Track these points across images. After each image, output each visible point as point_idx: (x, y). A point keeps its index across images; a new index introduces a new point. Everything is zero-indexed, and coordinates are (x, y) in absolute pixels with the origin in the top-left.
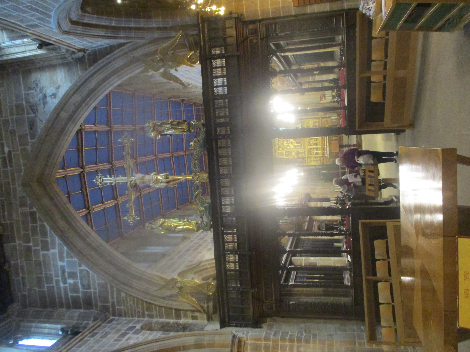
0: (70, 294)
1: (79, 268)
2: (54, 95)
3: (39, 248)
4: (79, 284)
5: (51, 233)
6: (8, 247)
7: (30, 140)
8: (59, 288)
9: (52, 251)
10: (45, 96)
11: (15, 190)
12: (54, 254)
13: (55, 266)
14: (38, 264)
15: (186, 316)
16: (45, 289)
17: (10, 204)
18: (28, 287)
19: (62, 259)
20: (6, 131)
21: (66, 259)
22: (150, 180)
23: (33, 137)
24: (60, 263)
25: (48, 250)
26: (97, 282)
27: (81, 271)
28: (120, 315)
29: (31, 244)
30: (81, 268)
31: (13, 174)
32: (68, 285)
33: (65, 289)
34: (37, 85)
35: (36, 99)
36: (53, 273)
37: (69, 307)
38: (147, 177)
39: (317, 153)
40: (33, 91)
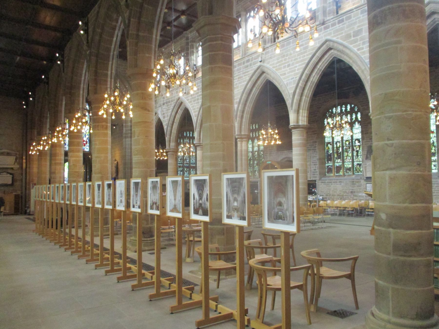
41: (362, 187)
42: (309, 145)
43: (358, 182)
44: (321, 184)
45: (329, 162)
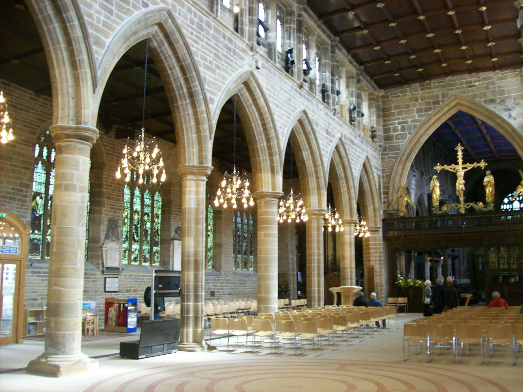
0: (392, 127)
1: (408, 132)
2: (510, 116)
3: (418, 107)
4: (397, 133)
5: (427, 114)
6: (417, 85)
7: (483, 100)
8: (395, 119)
9: (417, 115)
10: (509, 110)
11: (452, 90)
12: (414, 117)
13: (407, 118)
14: (408, 106)
15: (385, 198)
16: (393, 111)
17: (444, 86)
18: (394, 99)
19: (412, 121)
20: (488, 83)
21: (412, 124)
22: (460, 180)
23: (485, 102)
24: (409, 120)
25: (417, 112)
26: (400, 144)
27: (406, 134)
28: (382, 158)
29: (420, 101)
30: (408, 134)
31: (462, 88)
32: (397, 125)
33: (394, 124)
34: (517, 104)
35: (508, 104)
36: (404, 116)
37: (384, 126)
38: (462, 178)
39: (499, 264)
40: (513, 102)
41: (98, 282)
42: (13, 189)
43: (92, 275)
44: (33, 276)
45: (36, 232)
